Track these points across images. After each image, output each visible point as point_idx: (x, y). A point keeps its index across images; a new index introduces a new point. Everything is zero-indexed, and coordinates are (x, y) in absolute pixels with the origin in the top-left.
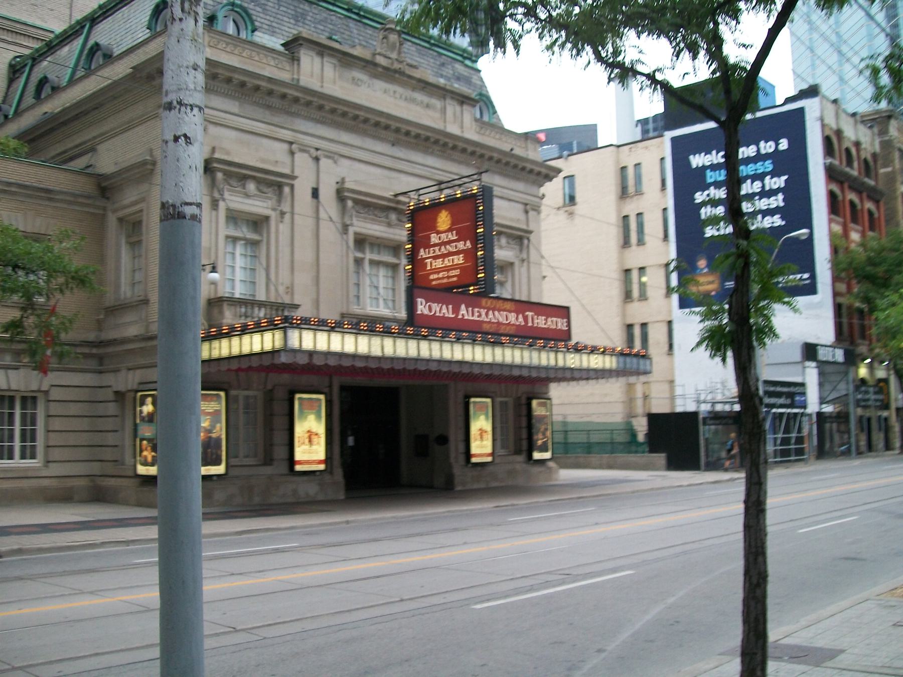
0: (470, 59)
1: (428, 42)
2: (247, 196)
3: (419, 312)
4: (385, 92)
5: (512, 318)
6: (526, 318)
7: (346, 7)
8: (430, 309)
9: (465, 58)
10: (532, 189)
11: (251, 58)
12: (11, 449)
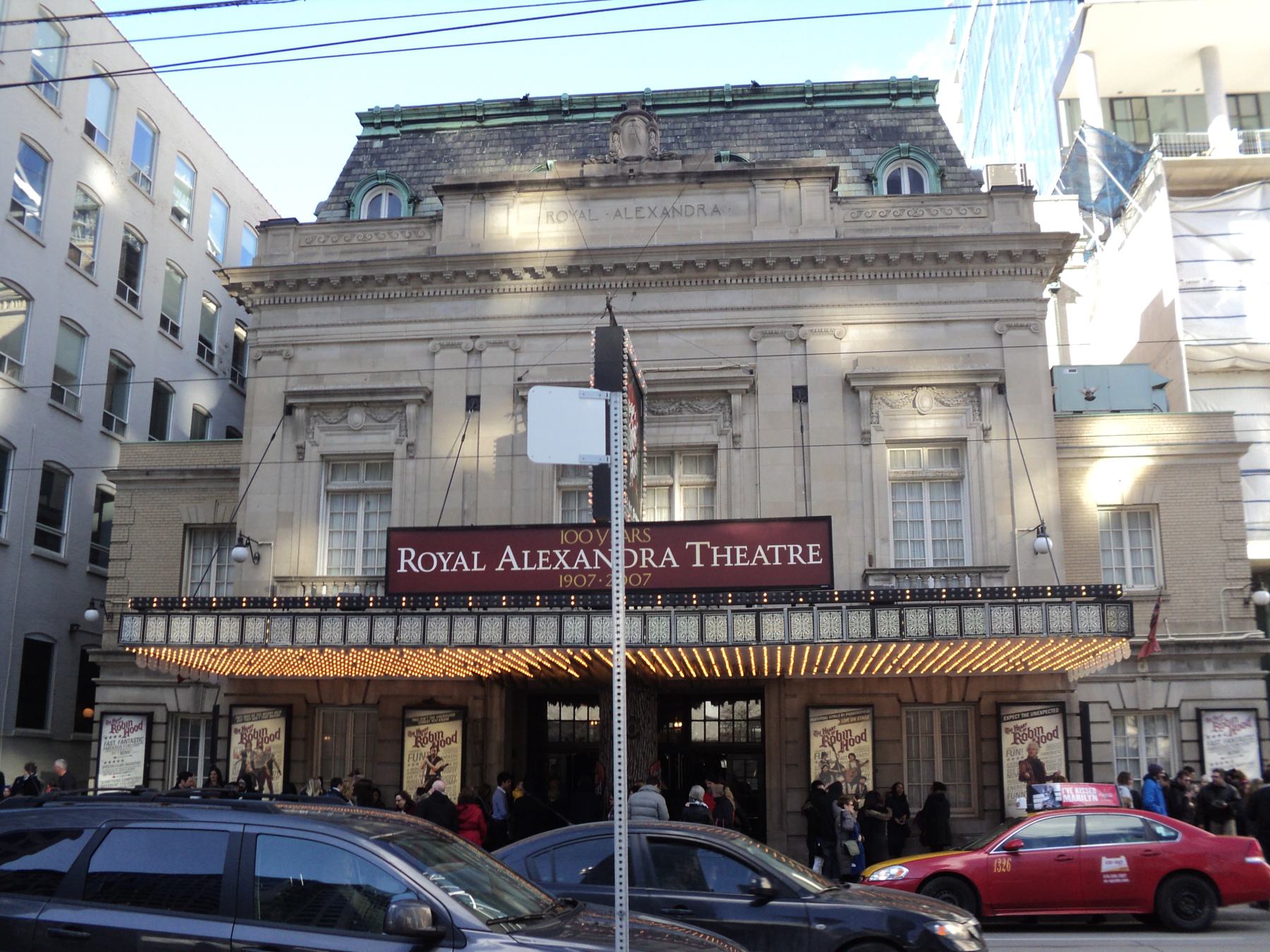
0: (909, 95)
1: (802, 100)
2: (358, 431)
4: (618, 214)
6: (685, 557)
7: (618, 105)
8: (427, 562)
9: (895, 98)
10: (1022, 286)
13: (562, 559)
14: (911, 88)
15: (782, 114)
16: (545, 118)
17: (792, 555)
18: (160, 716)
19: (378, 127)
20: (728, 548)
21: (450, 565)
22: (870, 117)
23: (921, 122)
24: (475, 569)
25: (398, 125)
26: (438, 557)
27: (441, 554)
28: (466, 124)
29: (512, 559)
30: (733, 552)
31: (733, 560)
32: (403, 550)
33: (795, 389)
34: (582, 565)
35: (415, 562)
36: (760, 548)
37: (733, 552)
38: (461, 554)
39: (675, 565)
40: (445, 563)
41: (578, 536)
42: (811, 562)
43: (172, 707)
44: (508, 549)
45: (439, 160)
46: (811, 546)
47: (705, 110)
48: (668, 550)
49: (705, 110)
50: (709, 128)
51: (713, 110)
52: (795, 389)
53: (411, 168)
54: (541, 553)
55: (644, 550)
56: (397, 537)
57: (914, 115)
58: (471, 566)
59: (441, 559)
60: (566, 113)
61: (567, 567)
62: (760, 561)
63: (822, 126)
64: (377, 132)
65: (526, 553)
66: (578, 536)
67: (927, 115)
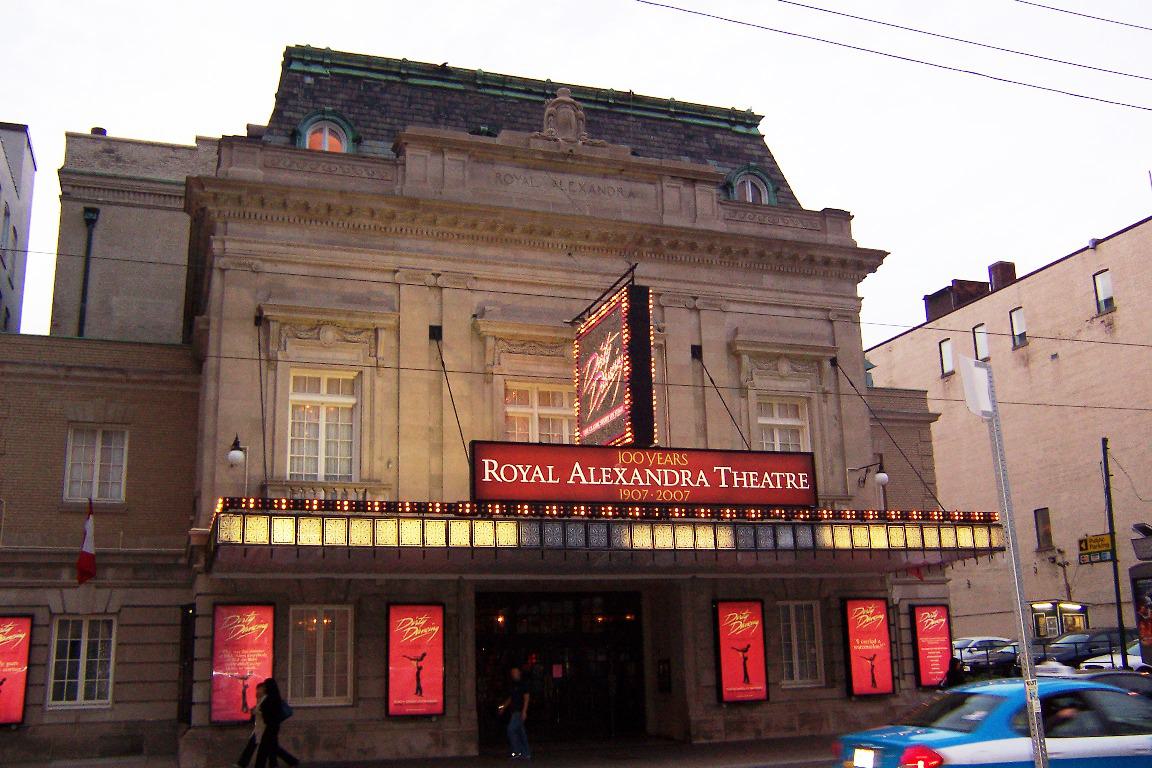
0: (742, 124)
3: (487, 479)
5: (685, 477)
6: (714, 478)
8: (509, 473)
9: (734, 124)
11: (330, 173)
12: (73, 688)
13: (621, 476)
14: (744, 118)
15: (652, 122)
16: (461, 87)
17: (789, 481)
18: (42, 616)
19: (307, 63)
20: (744, 473)
21: (529, 477)
22: (717, 136)
23: (753, 146)
24: (551, 481)
25: (326, 66)
26: (518, 470)
27: (520, 467)
28: (390, 78)
29: (581, 474)
30: (748, 477)
31: (749, 484)
32: (486, 461)
33: (693, 347)
34: (636, 481)
35: (498, 472)
36: (766, 475)
37: (748, 477)
38: (537, 468)
39: (707, 485)
40: (524, 474)
41: (633, 458)
42: (802, 487)
43: (57, 608)
44: (577, 465)
45: (372, 107)
46: (801, 475)
47: (592, 106)
48: (701, 473)
49: (592, 106)
50: (598, 122)
51: (598, 107)
52: (693, 347)
53: (345, 109)
54: (604, 470)
55: (683, 471)
56: (477, 450)
57: (747, 140)
58: (547, 478)
59: (520, 471)
60: (479, 86)
61: (625, 483)
62: (767, 484)
63: (683, 136)
64: (306, 69)
65: (592, 469)
66: (633, 458)
67: (756, 142)
